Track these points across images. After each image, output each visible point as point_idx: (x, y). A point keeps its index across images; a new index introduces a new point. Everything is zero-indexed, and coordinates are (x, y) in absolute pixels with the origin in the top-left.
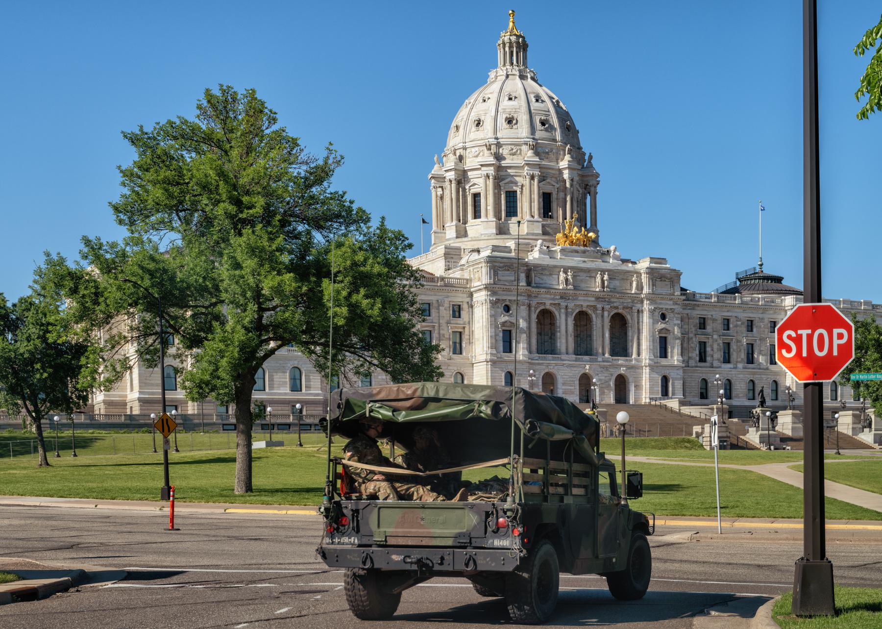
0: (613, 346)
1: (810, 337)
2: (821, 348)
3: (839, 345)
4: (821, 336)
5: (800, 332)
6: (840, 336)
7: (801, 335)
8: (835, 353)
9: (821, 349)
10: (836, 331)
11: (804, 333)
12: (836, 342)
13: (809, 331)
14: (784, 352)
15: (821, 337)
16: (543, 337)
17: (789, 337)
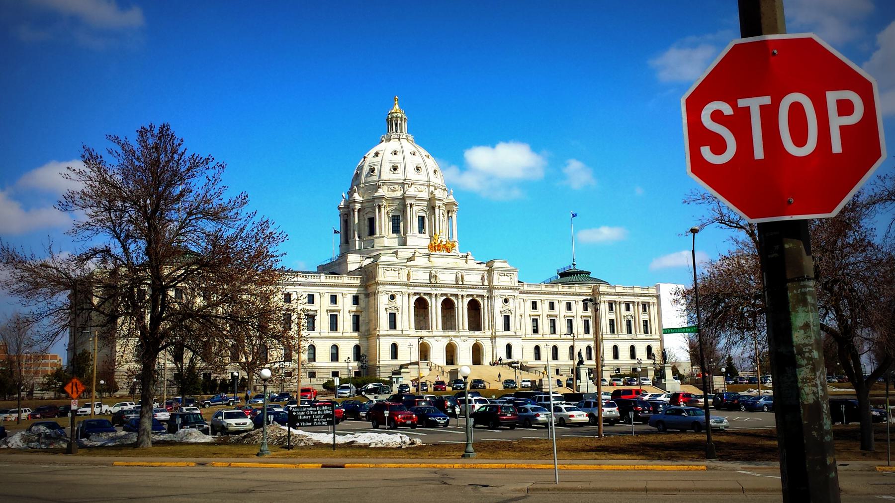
0: (470, 323)
1: (769, 115)
2: (800, 137)
3: (843, 129)
4: (796, 110)
5: (742, 103)
6: (845, 108)
7: (747, 110)
8: (837, 147)
9: (800, 139)
10: (832, 97)
11: (754, 104)
12: (836, 122)
13: (767, 100)
14: (706, 152)
15: (797, 113)
16: (419, 318)
17: (717, 116)
